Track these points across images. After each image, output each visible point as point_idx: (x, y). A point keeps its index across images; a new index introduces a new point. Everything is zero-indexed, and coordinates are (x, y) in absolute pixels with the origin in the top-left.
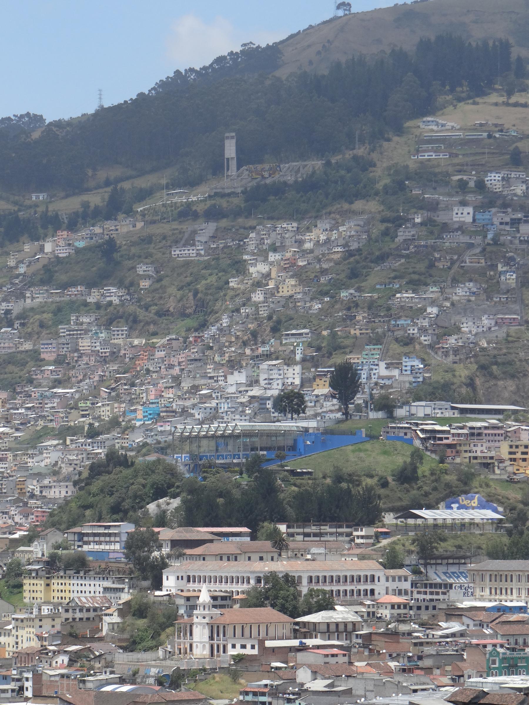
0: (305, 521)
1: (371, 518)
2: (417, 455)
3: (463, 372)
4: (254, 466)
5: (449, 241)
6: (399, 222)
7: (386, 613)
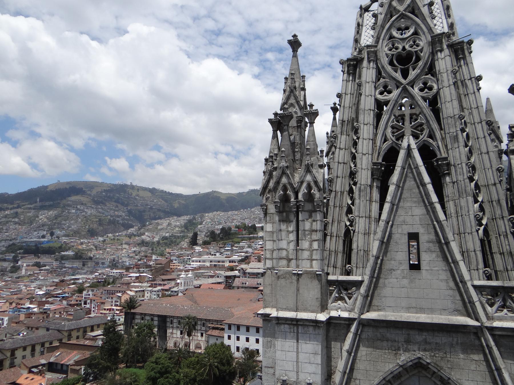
0: (43, 254)
1: (54, 253)
2: (62, 245)
3: (71, 233)
4: (36, 245)
5: (71, 215)
6: (63, 211)
7: (55, 267)
